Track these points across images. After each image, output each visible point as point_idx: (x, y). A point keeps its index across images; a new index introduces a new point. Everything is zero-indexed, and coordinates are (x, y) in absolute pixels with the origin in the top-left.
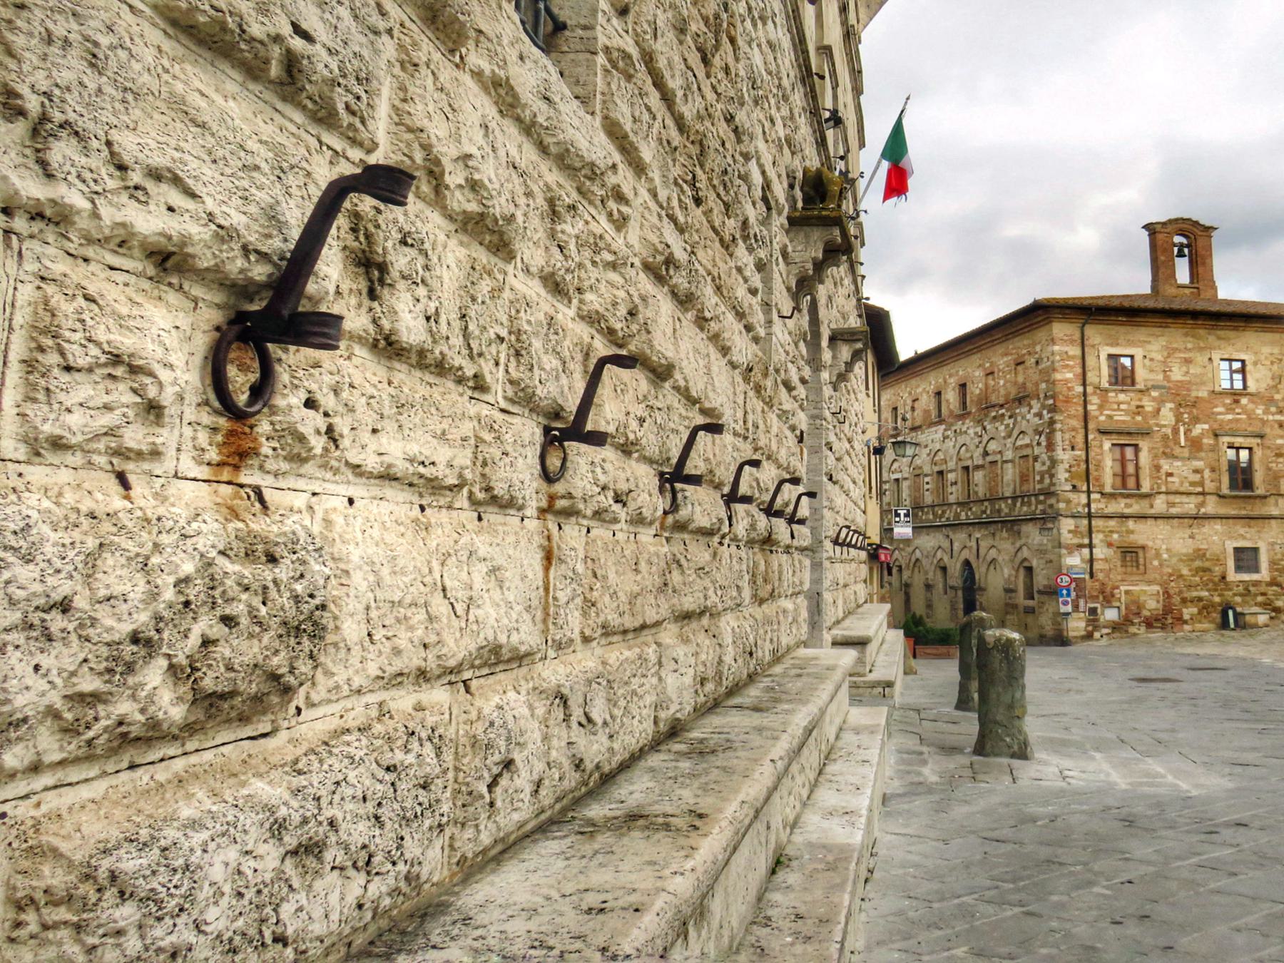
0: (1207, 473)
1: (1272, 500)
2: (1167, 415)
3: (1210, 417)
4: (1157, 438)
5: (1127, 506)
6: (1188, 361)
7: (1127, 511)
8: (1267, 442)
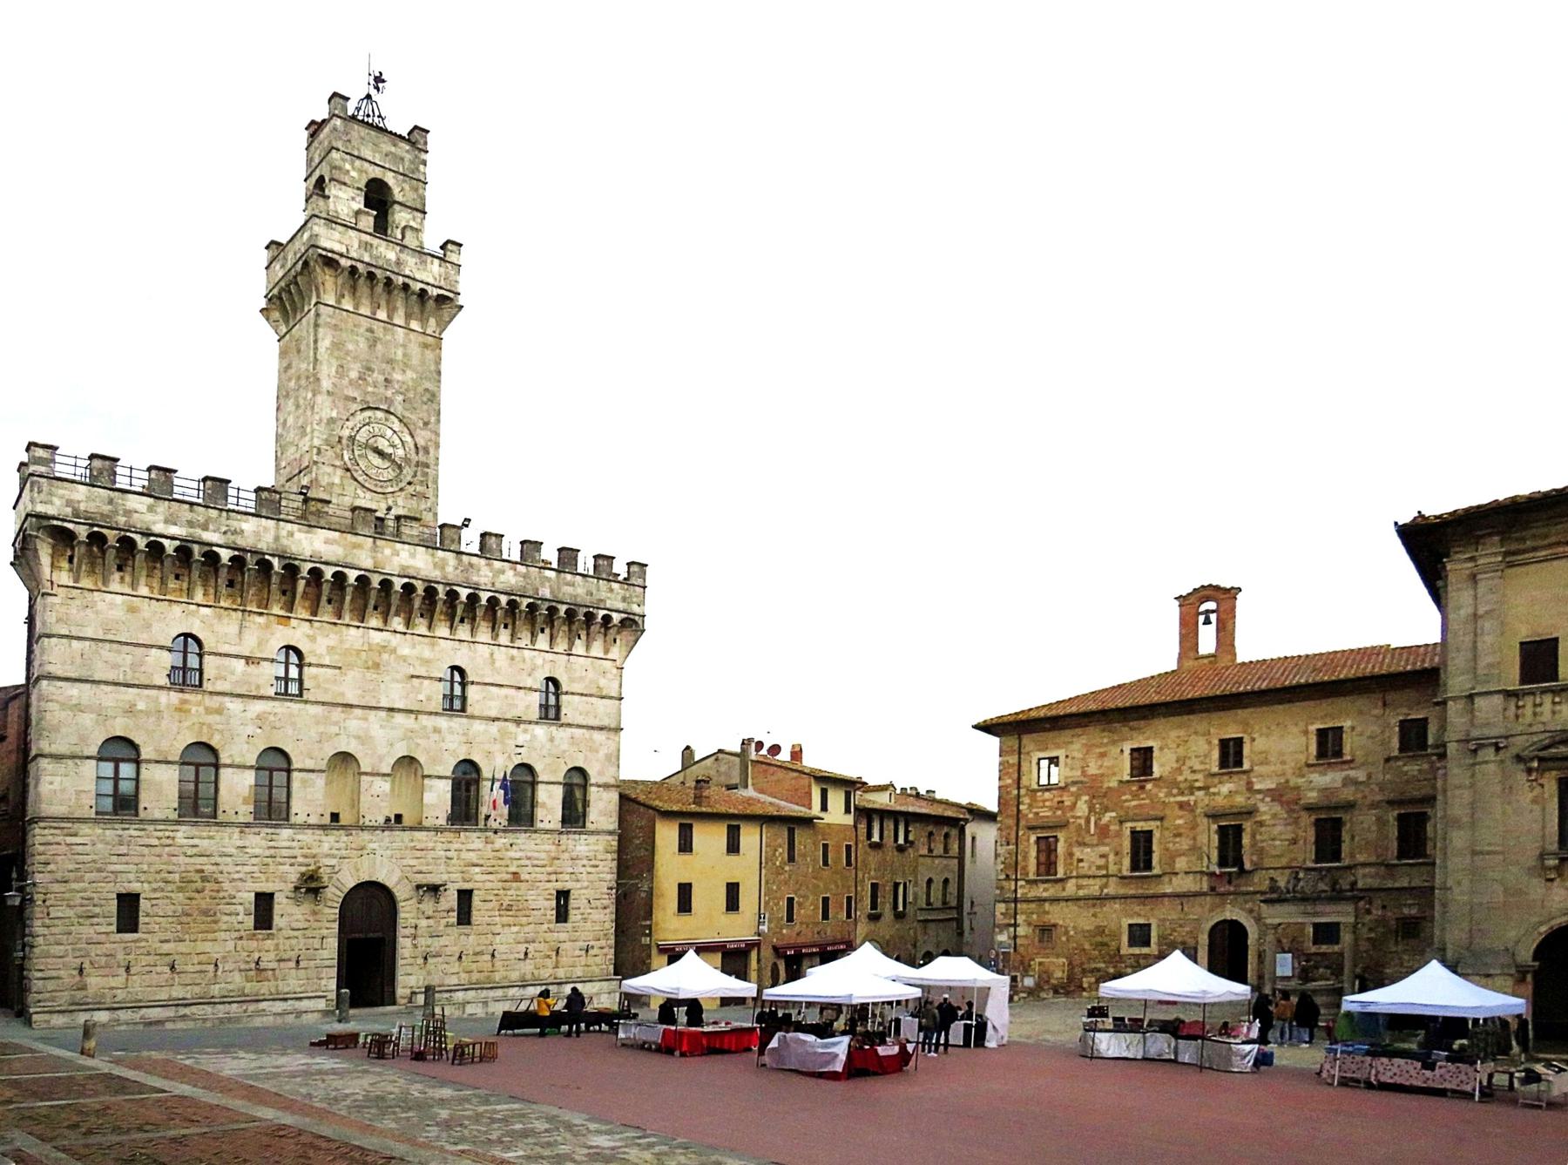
0: (1111, 857)
1: (1166, 879)
2: (1082, 808)
3: (1118, 806)
4: (1072, 828)
5: (1045, 890)
6: (1103, 755)
7: (1045, 895)
8: (1166, 824)
